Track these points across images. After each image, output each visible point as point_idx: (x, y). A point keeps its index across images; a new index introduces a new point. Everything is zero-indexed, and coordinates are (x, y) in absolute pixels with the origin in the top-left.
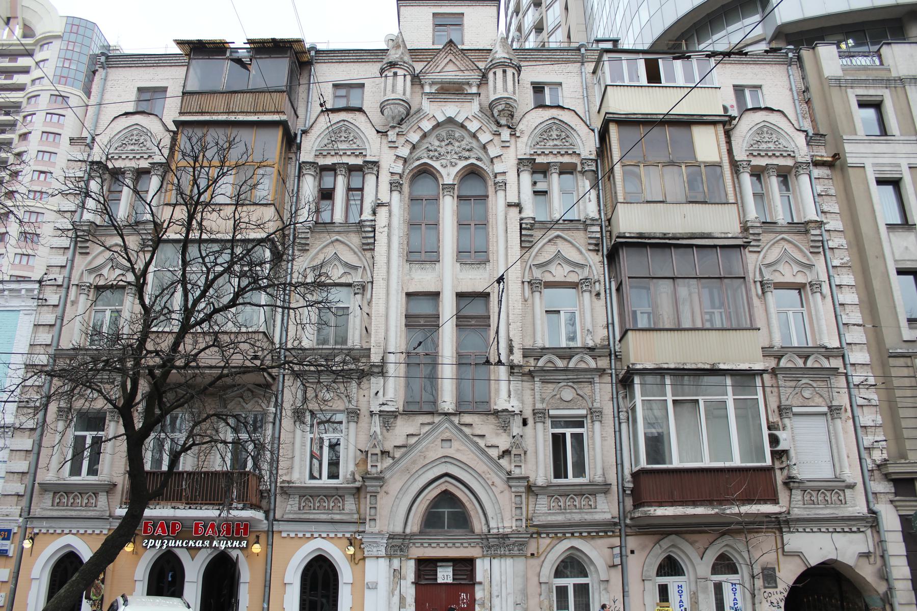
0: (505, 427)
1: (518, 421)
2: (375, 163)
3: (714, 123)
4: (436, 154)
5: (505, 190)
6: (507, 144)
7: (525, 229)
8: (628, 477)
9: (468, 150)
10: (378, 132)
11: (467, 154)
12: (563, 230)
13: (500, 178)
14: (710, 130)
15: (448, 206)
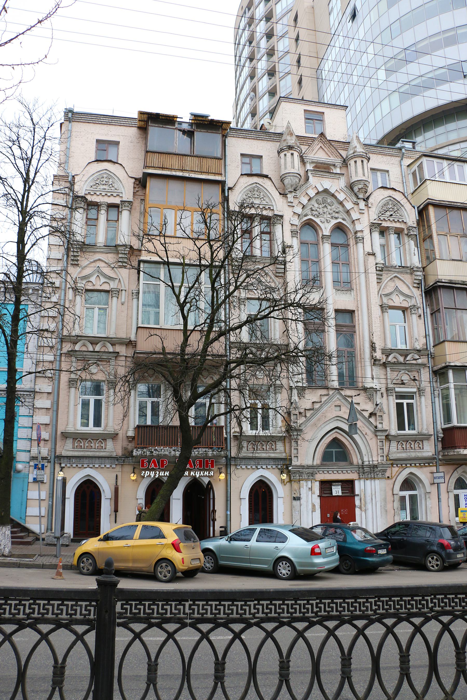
6: (363, 212)
12: (398, 272)
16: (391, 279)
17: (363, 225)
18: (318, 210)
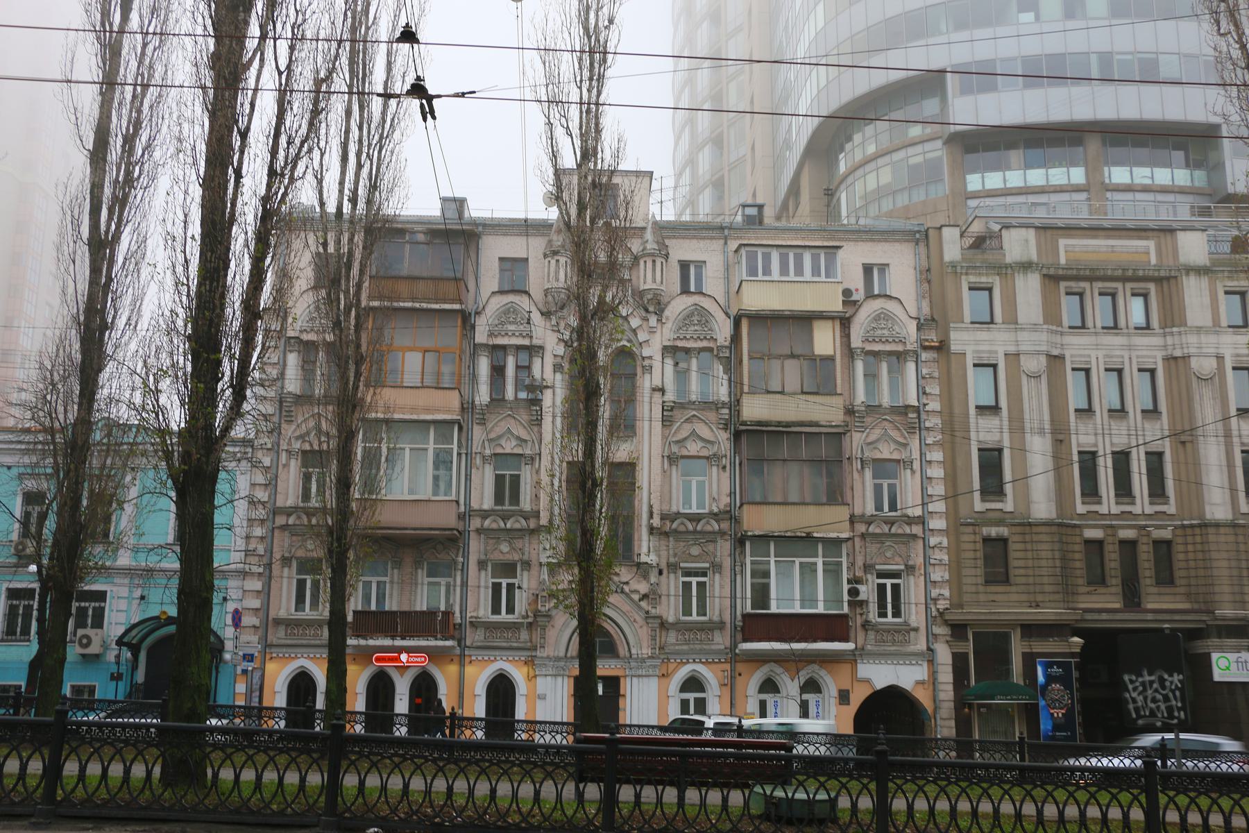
0: (645, 577)
1: (656, 571)
2: (542, 348)
3: (832, 318)
8: (739, 617)
14: (829, 324)
17: (653, 350)
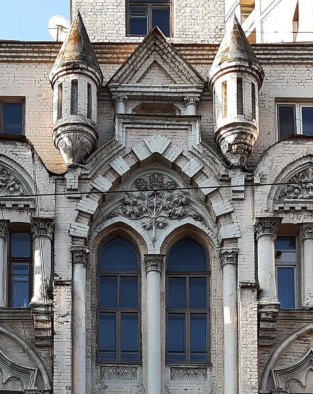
2: (50, 222)
4: (136, 210)
5: (236, 265)
6: (241, 196)
7: (265, 320)
9: (182, 204)
10: (51, 174)
11: (179, 210)
13: (228, 247)
15: (152, 287)
16: (299, 338)
18: (140, 202)
